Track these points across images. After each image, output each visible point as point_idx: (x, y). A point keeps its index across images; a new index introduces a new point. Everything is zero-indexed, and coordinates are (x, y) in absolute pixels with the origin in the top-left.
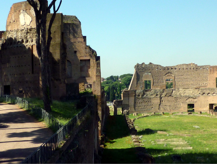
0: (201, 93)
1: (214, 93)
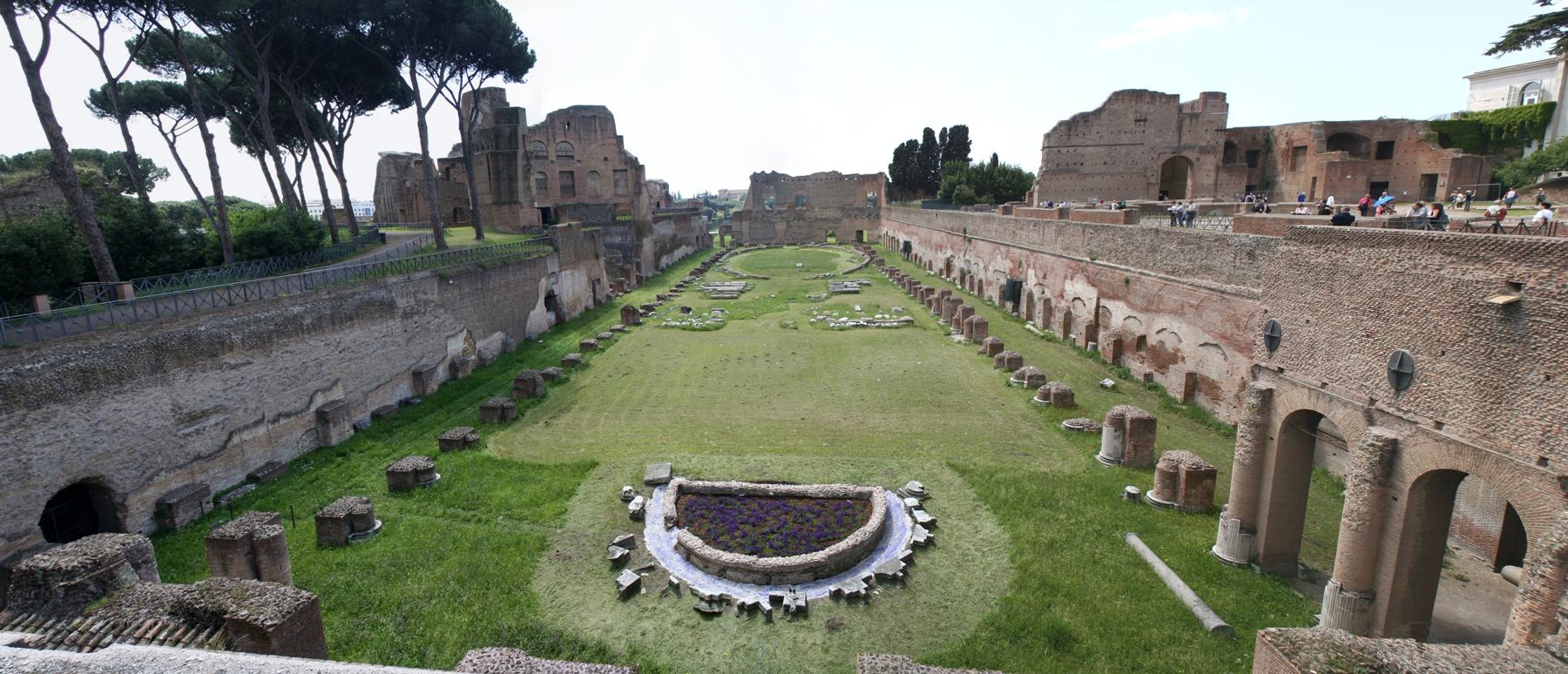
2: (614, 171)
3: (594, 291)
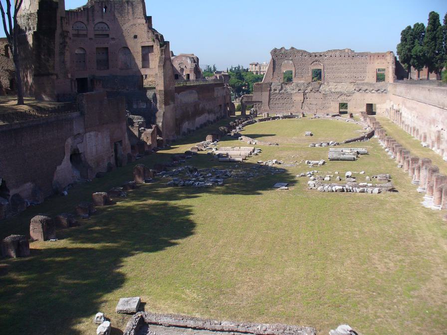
0: (357, 89)
1: (373, 90)
3: (116, 151)
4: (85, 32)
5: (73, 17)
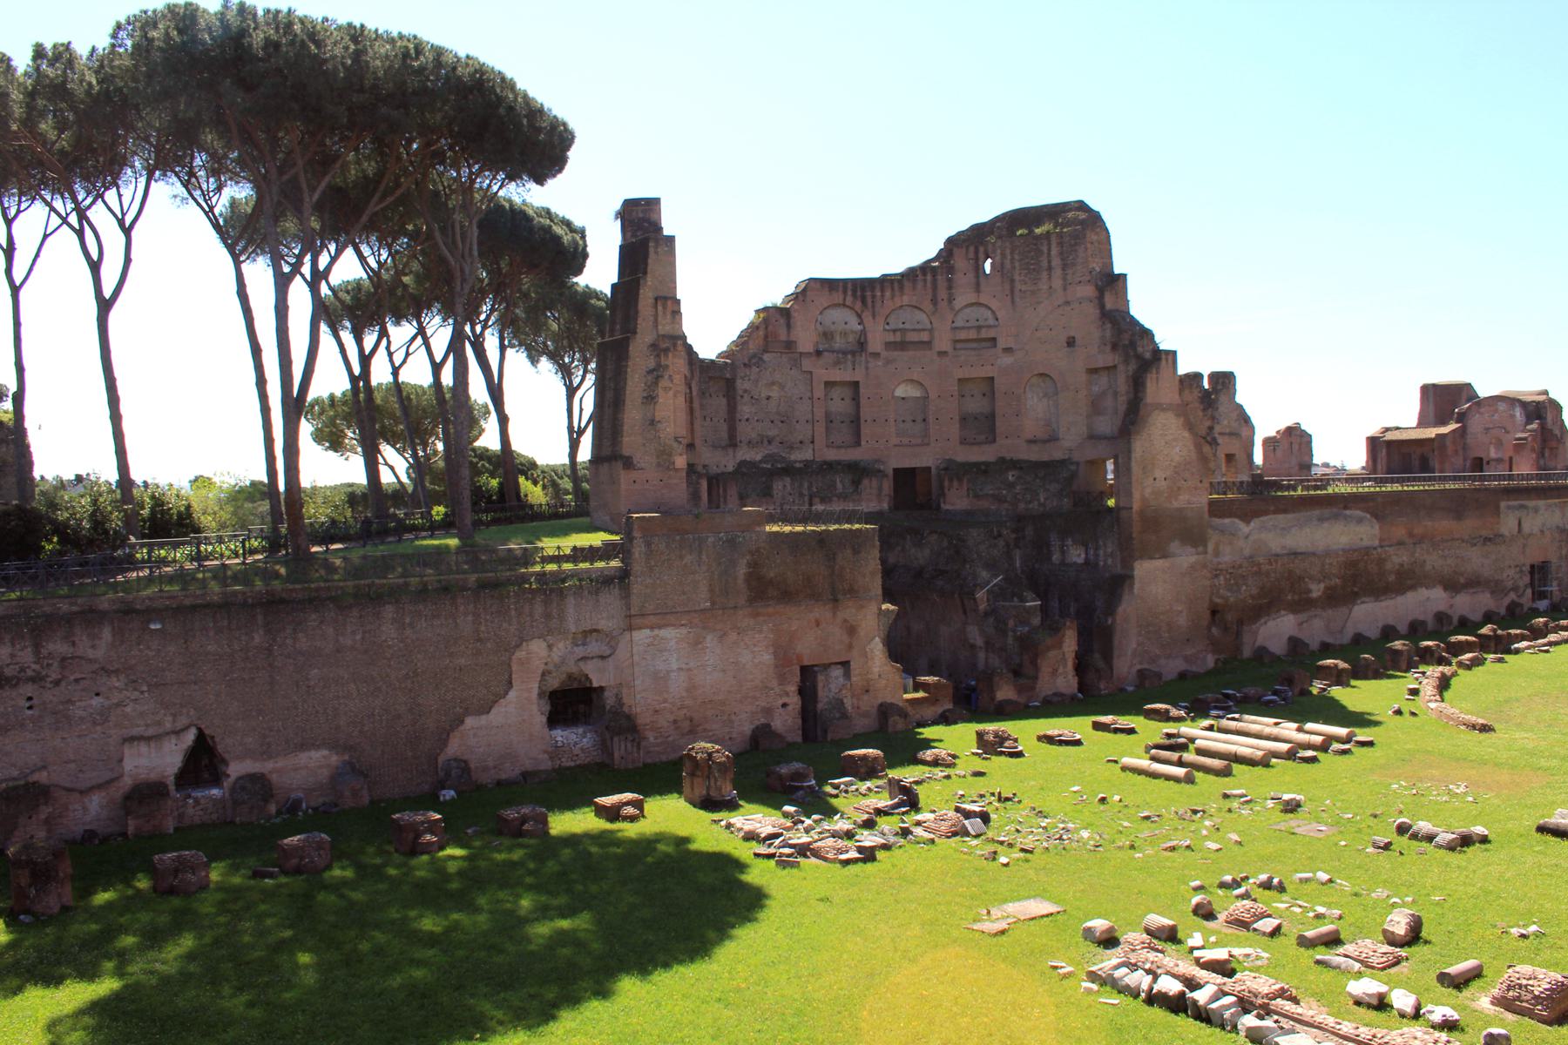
2: (1093, 371)
4: (925, 337)
5: (888, 294)
